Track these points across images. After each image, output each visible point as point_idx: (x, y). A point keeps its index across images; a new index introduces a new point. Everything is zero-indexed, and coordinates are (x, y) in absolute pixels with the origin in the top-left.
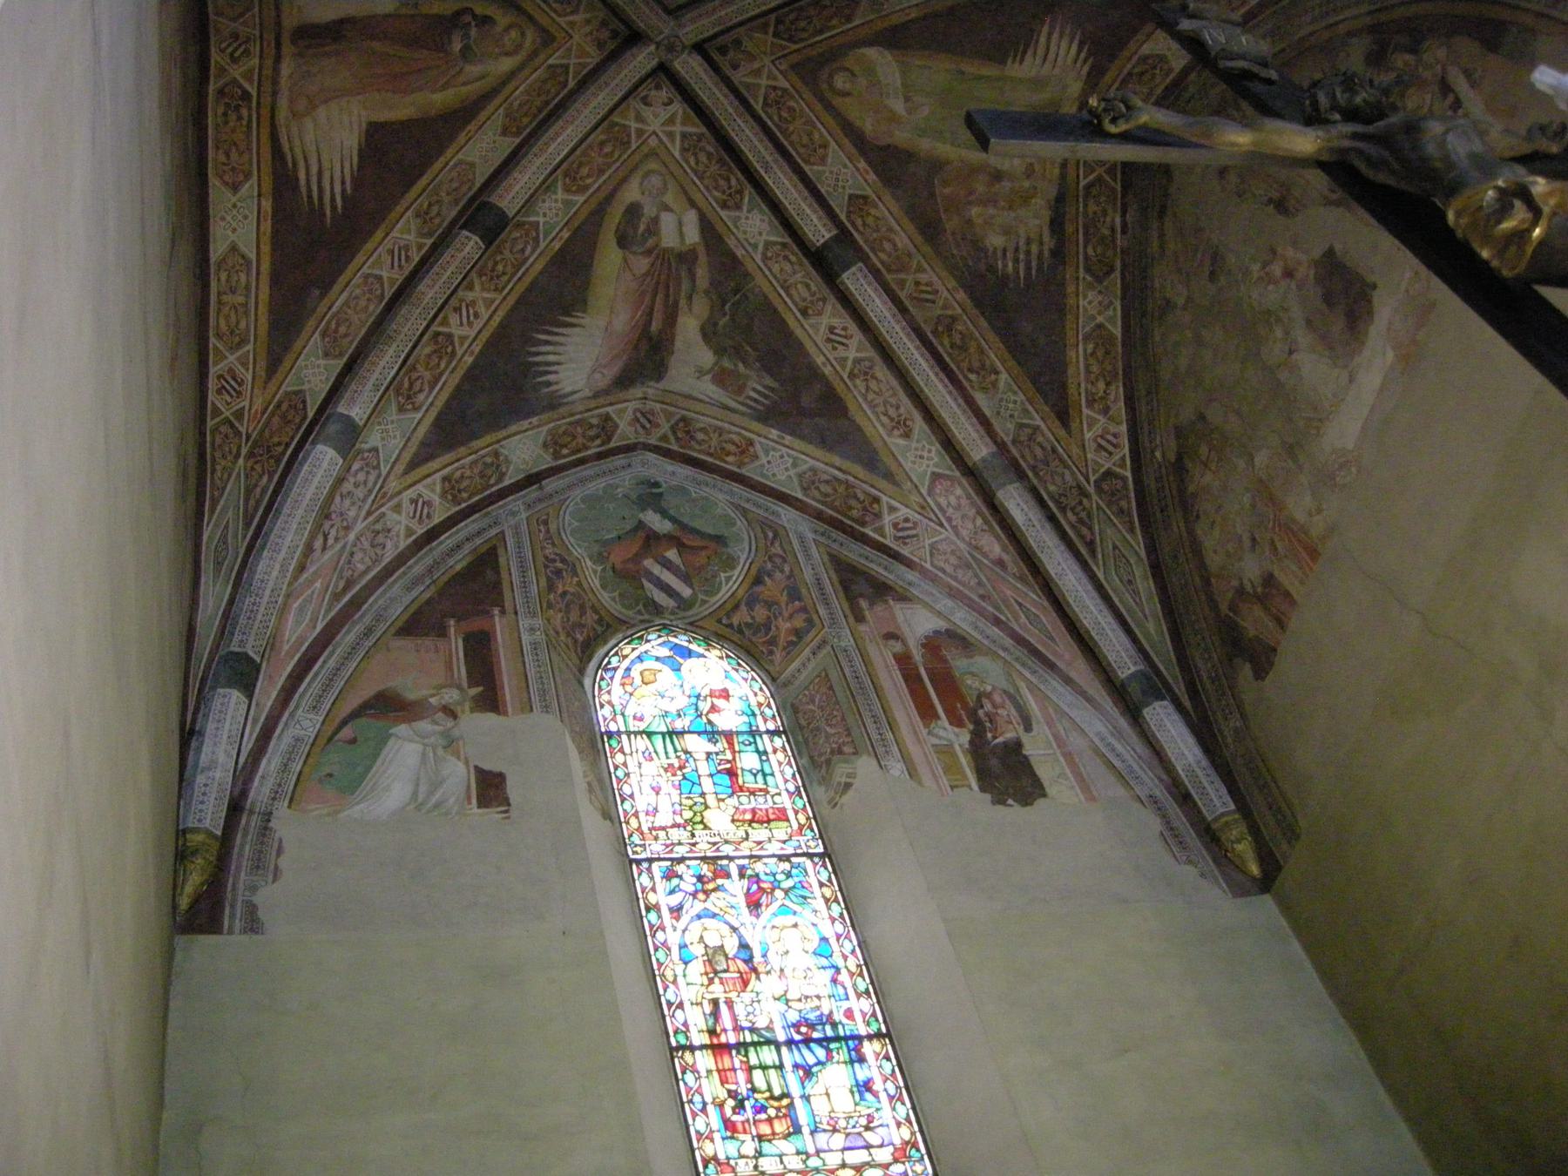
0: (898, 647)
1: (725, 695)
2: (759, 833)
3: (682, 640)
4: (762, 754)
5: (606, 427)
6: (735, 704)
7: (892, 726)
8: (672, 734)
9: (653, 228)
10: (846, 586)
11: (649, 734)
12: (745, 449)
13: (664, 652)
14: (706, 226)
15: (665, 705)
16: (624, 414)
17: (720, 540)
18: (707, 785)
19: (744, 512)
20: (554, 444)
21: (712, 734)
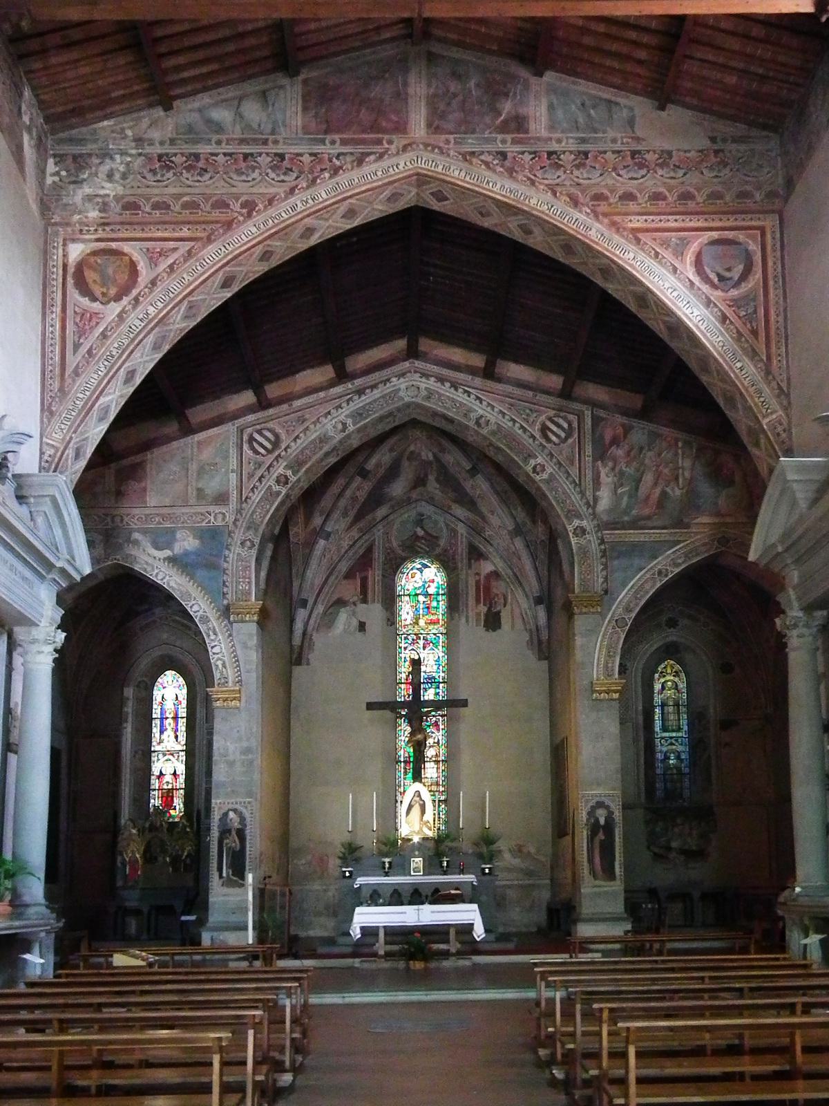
0: (477, 578)
1: (433, 581)
2: (431, 627)
3: (425, 562)
4: (438, 601)
5: (409, 499)
6: (435, 584)
7: (467, 607)
8: (417, 595)
9: (419, 454)
10: (470, 553)
11: (409, 595)
12: (450, 507)
13: (419, 566)
14: (435, 455)
15: (417, 585)
16: (414, 495)
17: (437, 538)
18: (421, 612)
19: (447, 525)
20: (392, 507)
21: (427, 595)
